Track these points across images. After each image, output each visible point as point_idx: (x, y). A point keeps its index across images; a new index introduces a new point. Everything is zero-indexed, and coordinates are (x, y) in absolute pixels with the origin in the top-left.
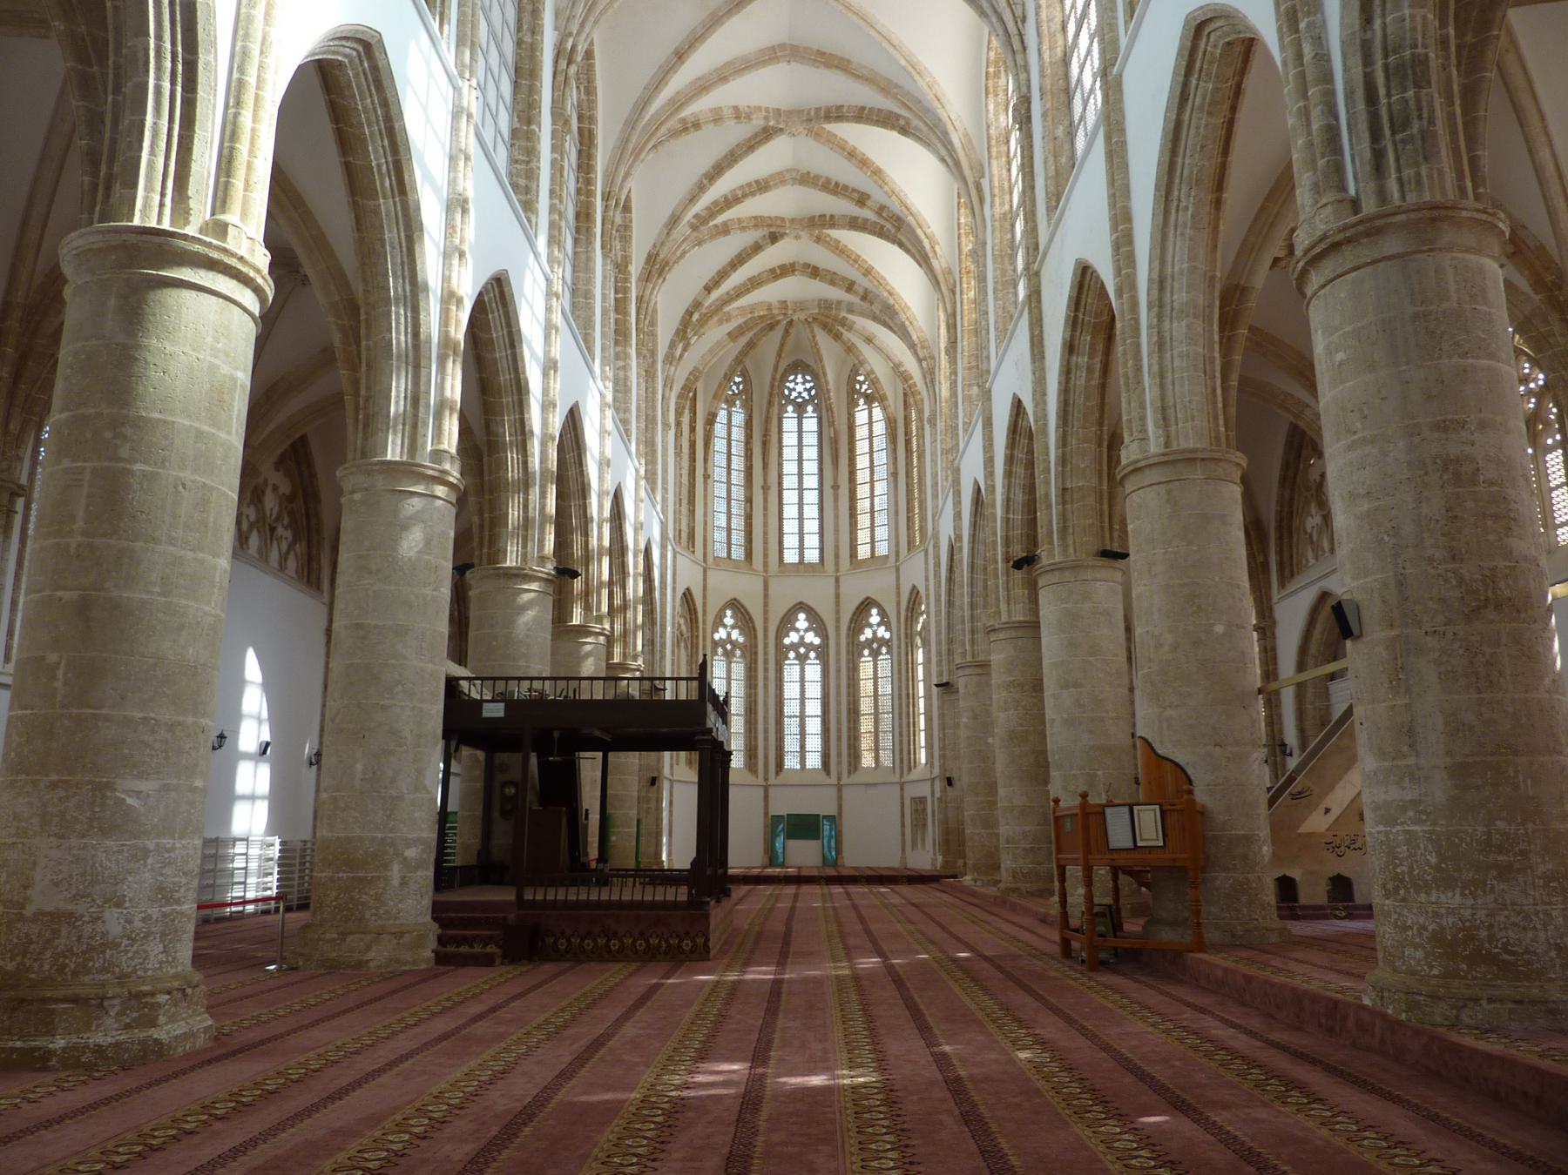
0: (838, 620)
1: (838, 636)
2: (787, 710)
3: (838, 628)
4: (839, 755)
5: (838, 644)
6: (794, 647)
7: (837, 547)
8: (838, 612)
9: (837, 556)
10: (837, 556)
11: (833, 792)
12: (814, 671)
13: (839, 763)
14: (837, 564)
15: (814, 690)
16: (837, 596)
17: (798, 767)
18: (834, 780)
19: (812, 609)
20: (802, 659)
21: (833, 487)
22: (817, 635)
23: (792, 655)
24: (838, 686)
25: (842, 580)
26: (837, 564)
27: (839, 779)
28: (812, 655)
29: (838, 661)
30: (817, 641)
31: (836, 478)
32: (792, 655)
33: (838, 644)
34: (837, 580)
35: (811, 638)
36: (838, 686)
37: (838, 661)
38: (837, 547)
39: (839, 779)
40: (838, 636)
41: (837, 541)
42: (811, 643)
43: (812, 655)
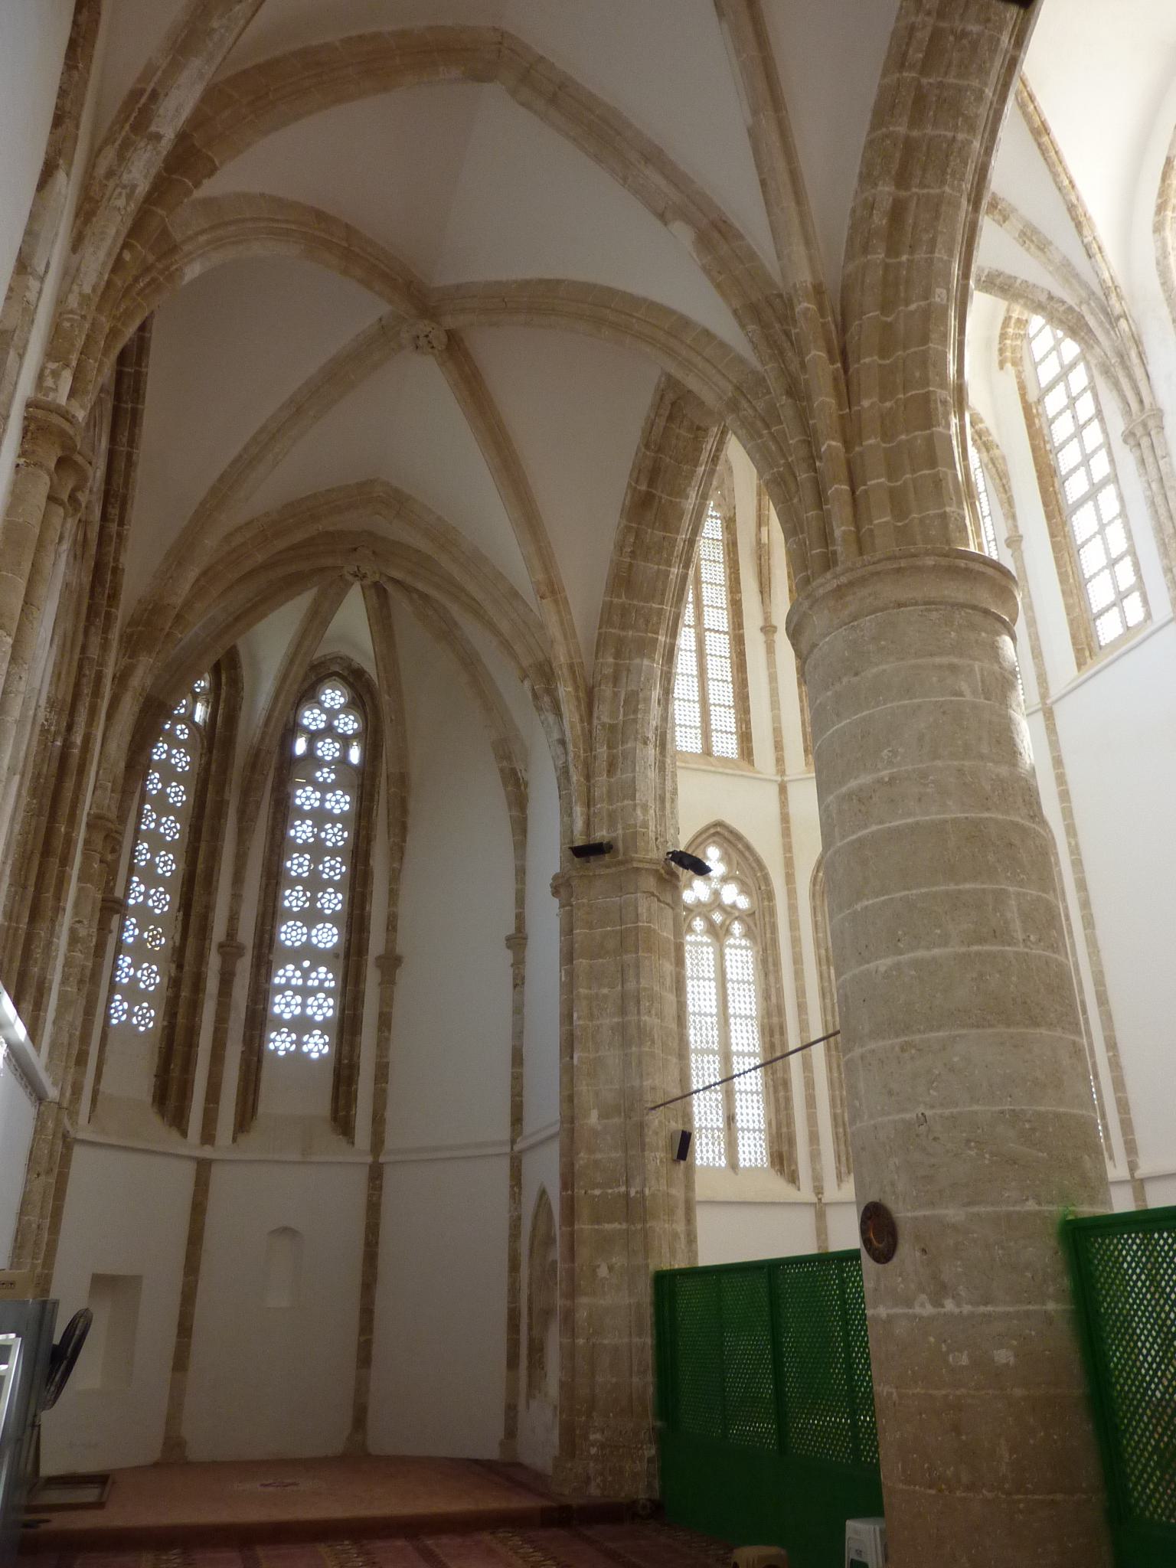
0: (789, 864)
1: (791, 893)
2: (694, 1038)
3: (790, 878)
4: (814, 1138)
5: (793, 908)
6: (702, 909)
7: (777, 732)
8: (788, 848)
9: (778, 746)
10: (778, 746)
11: (808, 1217)
12: (741, 960)
13: (815, 1156)
14: (780, 761)
15: (745, 1002)
16: (785, 818)
17: (723, 1162)
18: (806, 1194)
19: (739, 837)
20: (718, 933)
21: (774, 629)
22: (745, 890)
23: (698, 924)
24: (801, 992)
25: (792, 789)
26: (780, 761)
27: (819, 1190)
28: (737, 928)
29: (796, 942)
30: (743, 903)
31: (767, 617)
32: (698, 924)
33: (793, 908)
34: (783, 789)
35: (731, 894)
36: (801, 992)
37: (796, 942)
38: (777, 732)
39: (819, 1190)
40: (791, 893)
41: (776, 720)
42: (734, 906)
43: (737, 928)
